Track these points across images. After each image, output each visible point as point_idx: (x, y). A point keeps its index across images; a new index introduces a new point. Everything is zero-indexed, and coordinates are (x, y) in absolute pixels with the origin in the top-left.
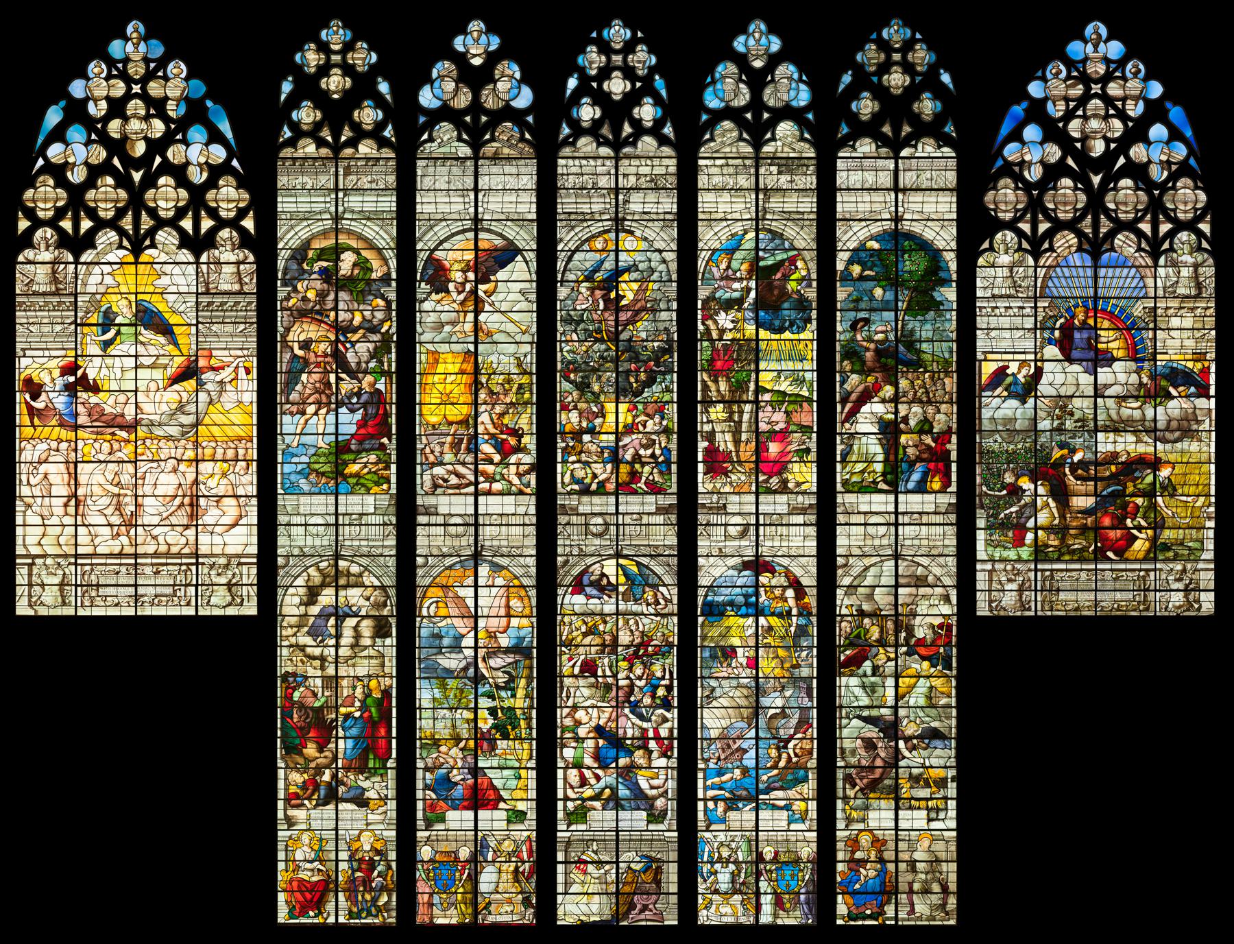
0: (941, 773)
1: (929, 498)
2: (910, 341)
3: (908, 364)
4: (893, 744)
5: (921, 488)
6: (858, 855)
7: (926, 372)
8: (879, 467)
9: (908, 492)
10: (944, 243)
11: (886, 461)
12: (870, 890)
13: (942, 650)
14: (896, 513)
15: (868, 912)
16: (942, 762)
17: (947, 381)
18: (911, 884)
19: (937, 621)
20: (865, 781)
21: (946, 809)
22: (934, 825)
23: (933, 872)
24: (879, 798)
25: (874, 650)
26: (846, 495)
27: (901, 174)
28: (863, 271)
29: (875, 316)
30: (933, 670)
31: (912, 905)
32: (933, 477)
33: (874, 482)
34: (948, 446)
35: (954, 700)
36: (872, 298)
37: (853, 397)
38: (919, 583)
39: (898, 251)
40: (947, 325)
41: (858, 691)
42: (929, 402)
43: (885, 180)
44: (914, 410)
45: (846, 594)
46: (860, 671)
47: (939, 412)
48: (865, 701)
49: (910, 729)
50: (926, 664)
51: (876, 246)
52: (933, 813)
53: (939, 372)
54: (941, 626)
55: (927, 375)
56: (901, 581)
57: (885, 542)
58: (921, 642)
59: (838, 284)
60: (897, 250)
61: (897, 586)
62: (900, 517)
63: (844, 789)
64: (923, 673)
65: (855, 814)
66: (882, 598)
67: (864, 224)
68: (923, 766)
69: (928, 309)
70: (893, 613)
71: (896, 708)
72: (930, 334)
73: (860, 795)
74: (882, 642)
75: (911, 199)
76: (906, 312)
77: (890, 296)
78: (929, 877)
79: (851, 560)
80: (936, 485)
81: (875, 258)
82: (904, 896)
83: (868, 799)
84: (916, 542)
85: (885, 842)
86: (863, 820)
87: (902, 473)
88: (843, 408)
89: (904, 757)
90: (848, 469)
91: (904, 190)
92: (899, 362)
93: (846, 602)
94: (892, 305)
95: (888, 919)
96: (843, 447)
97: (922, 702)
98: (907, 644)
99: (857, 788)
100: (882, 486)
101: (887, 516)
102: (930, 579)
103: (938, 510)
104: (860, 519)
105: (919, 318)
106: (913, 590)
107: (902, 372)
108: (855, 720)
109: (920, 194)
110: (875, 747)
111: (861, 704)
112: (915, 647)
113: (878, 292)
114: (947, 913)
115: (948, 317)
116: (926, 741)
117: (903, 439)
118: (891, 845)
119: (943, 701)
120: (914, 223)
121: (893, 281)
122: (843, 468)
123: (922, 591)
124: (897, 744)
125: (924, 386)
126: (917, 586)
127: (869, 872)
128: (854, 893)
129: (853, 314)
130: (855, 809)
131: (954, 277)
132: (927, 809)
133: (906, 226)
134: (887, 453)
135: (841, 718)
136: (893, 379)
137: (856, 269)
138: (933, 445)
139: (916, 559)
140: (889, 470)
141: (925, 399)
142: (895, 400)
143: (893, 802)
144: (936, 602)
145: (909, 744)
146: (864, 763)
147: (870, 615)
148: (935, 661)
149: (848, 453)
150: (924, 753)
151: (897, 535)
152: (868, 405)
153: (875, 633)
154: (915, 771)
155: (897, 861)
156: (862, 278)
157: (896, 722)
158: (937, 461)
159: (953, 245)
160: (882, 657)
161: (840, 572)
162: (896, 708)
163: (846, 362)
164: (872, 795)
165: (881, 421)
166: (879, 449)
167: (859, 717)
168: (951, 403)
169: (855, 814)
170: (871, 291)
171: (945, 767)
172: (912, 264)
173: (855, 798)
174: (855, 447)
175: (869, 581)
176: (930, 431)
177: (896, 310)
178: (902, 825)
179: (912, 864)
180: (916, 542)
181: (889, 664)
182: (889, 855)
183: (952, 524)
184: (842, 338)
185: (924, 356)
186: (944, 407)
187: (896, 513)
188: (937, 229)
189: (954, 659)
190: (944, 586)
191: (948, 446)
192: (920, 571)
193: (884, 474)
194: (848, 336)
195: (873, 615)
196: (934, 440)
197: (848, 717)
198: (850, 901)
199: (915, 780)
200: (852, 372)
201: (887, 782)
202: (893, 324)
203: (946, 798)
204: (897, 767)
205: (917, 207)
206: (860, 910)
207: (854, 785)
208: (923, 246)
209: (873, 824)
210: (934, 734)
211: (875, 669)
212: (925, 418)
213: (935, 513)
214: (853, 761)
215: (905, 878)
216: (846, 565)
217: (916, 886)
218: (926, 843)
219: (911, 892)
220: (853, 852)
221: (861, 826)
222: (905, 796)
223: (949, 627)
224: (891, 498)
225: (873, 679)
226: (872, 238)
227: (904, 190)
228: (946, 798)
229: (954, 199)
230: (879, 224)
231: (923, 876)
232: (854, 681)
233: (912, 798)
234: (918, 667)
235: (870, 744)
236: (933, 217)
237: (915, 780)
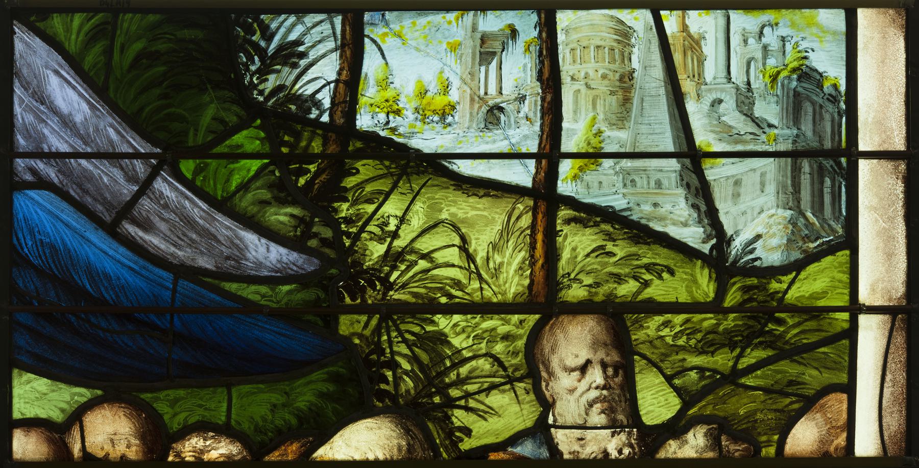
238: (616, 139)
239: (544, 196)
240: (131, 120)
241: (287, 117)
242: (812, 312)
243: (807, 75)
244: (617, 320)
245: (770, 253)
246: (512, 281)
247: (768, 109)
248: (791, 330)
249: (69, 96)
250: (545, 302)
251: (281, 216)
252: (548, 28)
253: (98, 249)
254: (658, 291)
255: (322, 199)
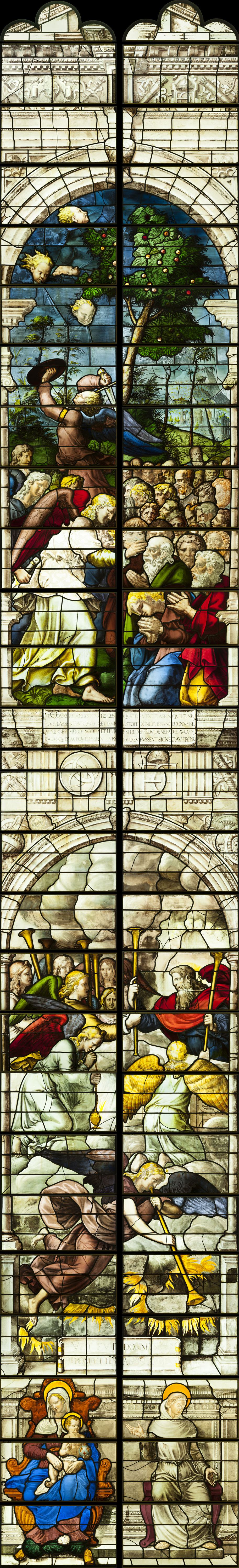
0: (208, 1264)
1: (184, 718)
2: (144, 405)
3: (142, 451)
4: (112, 1206)
5: (168, 699)
6: (45, 1427)
7: (177, 467)
8: (85, 658)
9: (142, 706)
10: (213, 211)
11: (98, 645)
12: (67, 1497)
13: (209, 1019)
14: (119, 748)
15: (64, 1540)
16: (209, 1243)
17: (219, 485)
18: (147, 1485)
19: (200, 962)
20: (57, 1280)
21: (218, 1336)
22: (193, 1367)
23: (192, 1460)
24: (86, 1315)
25: (75, 1020)
26: (21, 713)
27: (128, 82)
28: (53, 266)
29: (77, 357)
30: (191, 1059)
31: (150, 1527)
32: (191, 676)
33: (76, 687)
34: (221, 616)
35: (233, 1118)
36: (71, 320)
37: (34, 517)
38: (163, 887)
39: (122, 226)
40: (219, 375)
41: (44, 1102)
42: (184, 527)
43: (98, 89)
44: (153, 543)
45: (19, 908)
46: (48, 1062)
47: (203, 547)
48: (58, 1121)
49: (146, 1177)
50: (177, 1048)
51: (78, 215)
52: (192, 1345)
53: (204, 467)
54: (207, 972)
55: (179, 474)
56: (129, 882)
57: (97, 804)
58: (168, 1004)
59: (5, 292)
60: (119, 225)
61: (120, 892)
62: (127, 756)
63: (16, 1295)
64: (173, 1066)
65: (37, 1346)
66: (92, 916)
67: (55, 172)
68: (173, 1251)
69: (182, 343)
70: (112, 945)
71: (118, 1134)
72: (186, 393)
73: (47, 1308)
74: (90, 1005)
75: (149, 123)
76: (139, 346)
77: (106, 316)
78: (184, 1470)
79: (30, 841)
80: (198, 692)
81: (78, 241)
82: (135, 1508)
83: (62, 1315)
84: (158, 805)
85: (96, 1402)
86: (54, 1358)
87: (131, 668)
88: (14, 540)
89: (134, 1233)
90: (22, 662)
91: (135, 107)
92: (123, 446)
93: (21, 923)
94: (112, 335)
95: (104, 1554)
96: (14, 616)
97: (170, 1122)
98: (140, 1007)
99: (42, 1294)
100: (92, 695)
101: (100, 754)
102: (187, 878)
103: (202, 742)
104: (48, 760)
105: (164, 360)
106: (152, 901)
107: (131, 468)
108: (39, 1158)
109: (167, 113)
110: (77, 1213)
111: (50, 1126)
112: (157, 1014)
113: (84, 309)
114: (219, 1543)
115: (221, 358)
116: (179, 1201)
117: (133, 600)
118: (109, 1407)
119: (212, 1121)
120: (154, 172)
121: (115, 289)
122: (15, 659)
123: (170, 902)
124: (120, 1206)
125: (173, 495)
126: (160, 893)
127: (66, 1461)
128: (35, 1503)
129: (34, 351)
130: (38, 1337)
131: (233, 278)
132: (180, 1335)
133: (137, 177)
134: (100, 629)
135: (10, 1155)
136: (112, 482)
137: (40, 263)
138: (192, 612)
139: (158, 839)
140: (104, 662)
141: (175, 522)
142: (117, 523)
143: (113, 1322)
144: (198, 925)
145: (145, 1206)
146: (55, 1243)
147: (67, 950)
148: (194, 1042)
149: (24, 629)
150: (174, 1224)
151: (120, 791)
152: (64, 533)
153: (77, 987)
154: (157, 1261)
155: (120, 1440)
156: (50, 280)
157: (120, 1160)
158: (198, 644)
159: (231, 214)
160: (91, 1033)
161: (8, 864)
162: (118, 1134)
163: (19, 449)
164: (70, 1309)
165: (89, 566)
166: (84, 621)
167: (46, 1153)
168: (226, 528)
169: (37, 1346)
170: (69, 307)
171: (216, 1253)
172: (151, 254)
173: (38, 1314)
174: (39, 618)
175: (65, 883)
176: (185, 586)
177: (119, 344)
178: (131, 1366)
179: (150, 1444)
180: (158, 805)
181: (105, 1046)
182: (105, 1427)
183: (228, 770)
184: (12, 399)
185: (173, 435)
186: (212, 538)
187: (119, 748)
188: (200, 184)
189: (233, 1038)
190: (213, 893)
191: (221, 616)
192: (166, 862)
193: (95, 671)
194: (24, 395)
195: (72, 950)
196: (193, 604)
197: (24, 1154)
198: (28, 1519)
199: (157, 1278)
200: (33, 467)
201: (101, 1282)
202: (113, 372)
203: (217, 1315)
204: (121, 1253)
205: (159, 139)
206: (48, 1536)
207: (35, 1288)
208: (174, 216)
209: (72, 1366)
210: (192, 1188)
211: (78, 1059)
212: (177, 559)
213: (196, 748)
214: (34, 1240)
215: (135, 1473)
216: (19, 851)
217: (159, 1490)
218: (177, 1404)
219: (148, 1500)
220: (34, 1422)
221: (50, 1369)
222: (136, 1309)
223: (224, 973)
224: (109, 718)
225: (73, 1078)
226: (72, 201)
227: (135, 107)
228: (217, 1315)
229: (233, 124)
230: (85, 172)
231: (172, 1469)
232: (35, 1081)
233: (151, 1314)
234: (161, 1052)
235: (66, 1207)
236: (192, 158)
237: (157, 1278)
238: (200, 425)
239: (191, 432)
240: (139, 423)
241: (158, 422)
242: (225, 447)
243: (225, 417)
244: (201, 448)
245: (220, 440)
246: (187, 443)
247: (220, 421)
248: (223, 449)
249: (130, 419)
250: (191, 446)
251: (158, 435)
252: (192, 411)
253: (134, 439)
254: (206, 444)
255: (163, 433)
